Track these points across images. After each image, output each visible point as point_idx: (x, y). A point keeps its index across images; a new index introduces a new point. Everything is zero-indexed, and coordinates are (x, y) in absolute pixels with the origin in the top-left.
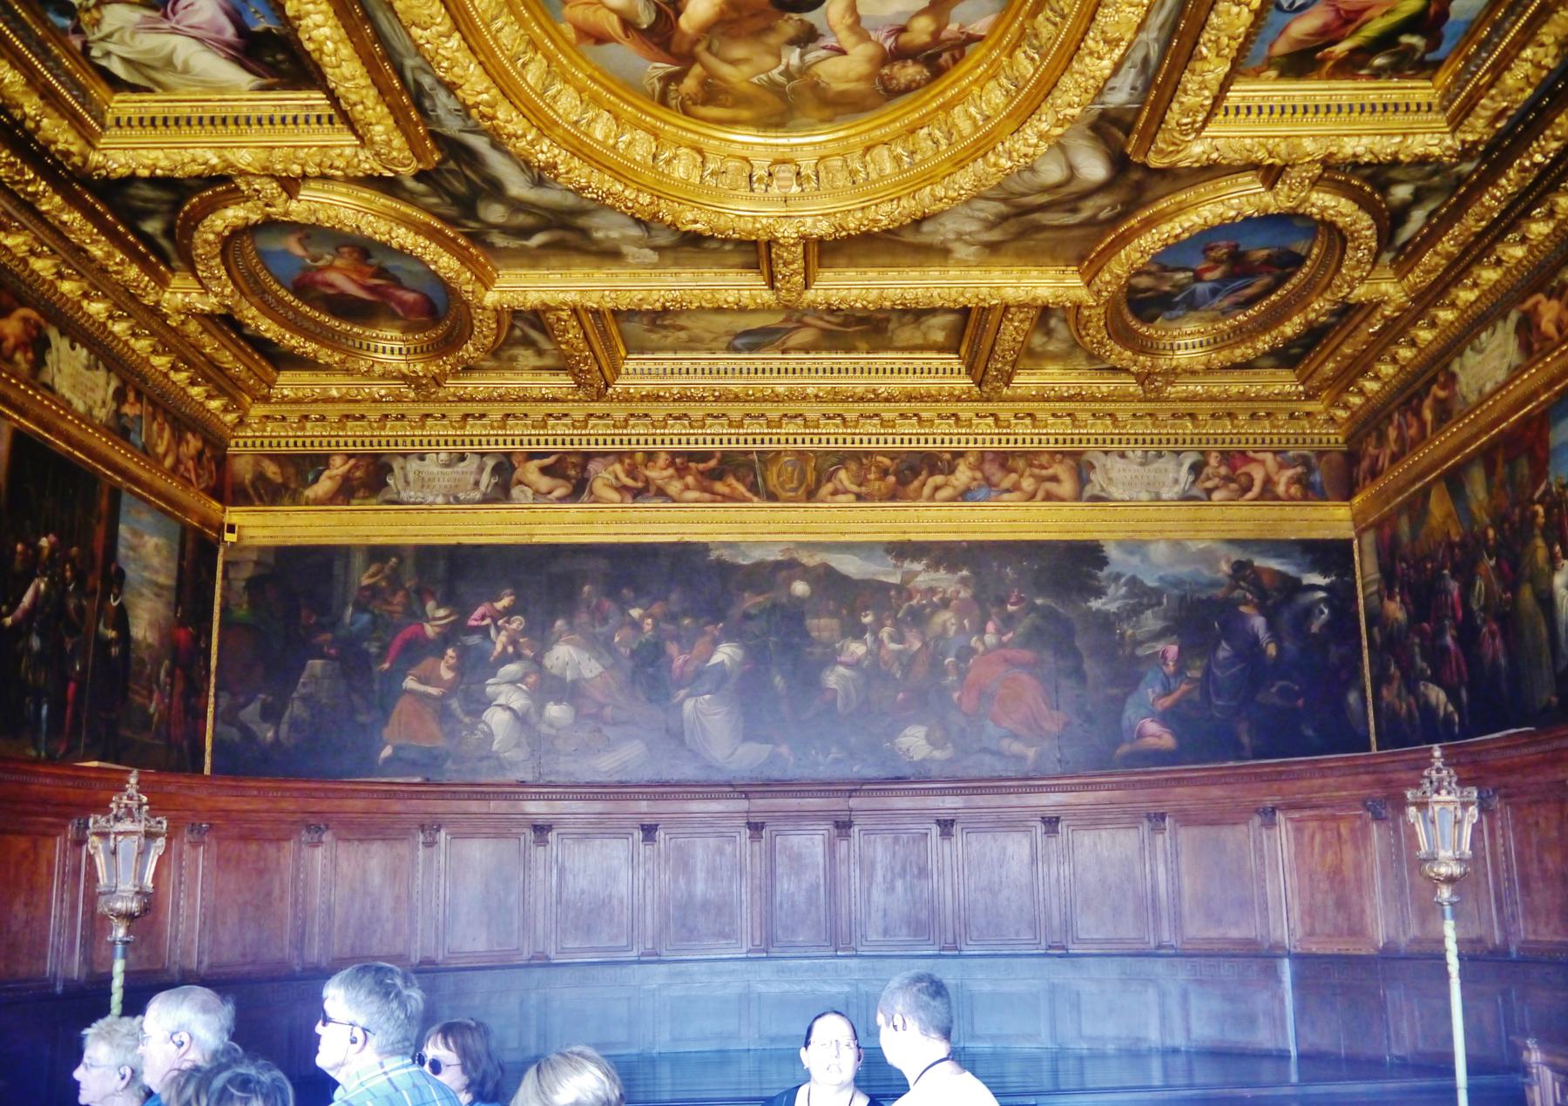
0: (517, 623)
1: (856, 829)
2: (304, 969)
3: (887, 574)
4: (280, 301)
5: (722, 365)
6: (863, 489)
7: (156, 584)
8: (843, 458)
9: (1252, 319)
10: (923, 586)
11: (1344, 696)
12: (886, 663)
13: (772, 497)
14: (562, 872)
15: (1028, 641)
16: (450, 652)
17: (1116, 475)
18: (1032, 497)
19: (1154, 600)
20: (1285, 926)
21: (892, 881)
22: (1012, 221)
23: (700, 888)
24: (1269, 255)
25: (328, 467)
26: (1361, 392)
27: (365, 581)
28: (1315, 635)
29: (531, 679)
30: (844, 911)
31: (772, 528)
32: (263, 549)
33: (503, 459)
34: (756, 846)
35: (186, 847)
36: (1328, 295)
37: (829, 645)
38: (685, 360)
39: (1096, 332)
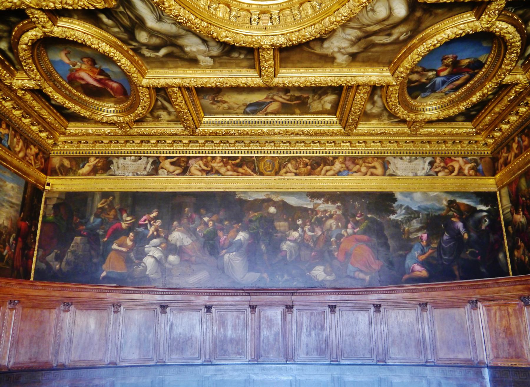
0: (159, 223)
1: (295, 309)
2: (57, 365)
3: (307, 204)
5: (242, 120)
6: (298, 171)
7: (11, 202)
8: (290, 159)
9: (458, 96)
10: (322, 209)
11: (497, 255)
12: (307, 240)
13: (261, 174)
14: (172, 325)
15: (364, 232)
16: (131, 234)
17: (400, 166)
18: (365, 174)
19: (416, 215)
20: (485, 354)
21: (310, 331)
22: (363, 41)
23: (229, 333)
24: (469, 62)
25: (88, 161)
26: (501, 130)
27: (100, 206)
28: (483, 230)
29: (163, 245)
30: (290, 344)
31: (261, 186)
32: (61, 193)
33: (156, 159)
34: (253, 316)
35: (7, 310)
36: (494, 80)
37: (284, 232)
38: (227, 118)
39: (394, 100)
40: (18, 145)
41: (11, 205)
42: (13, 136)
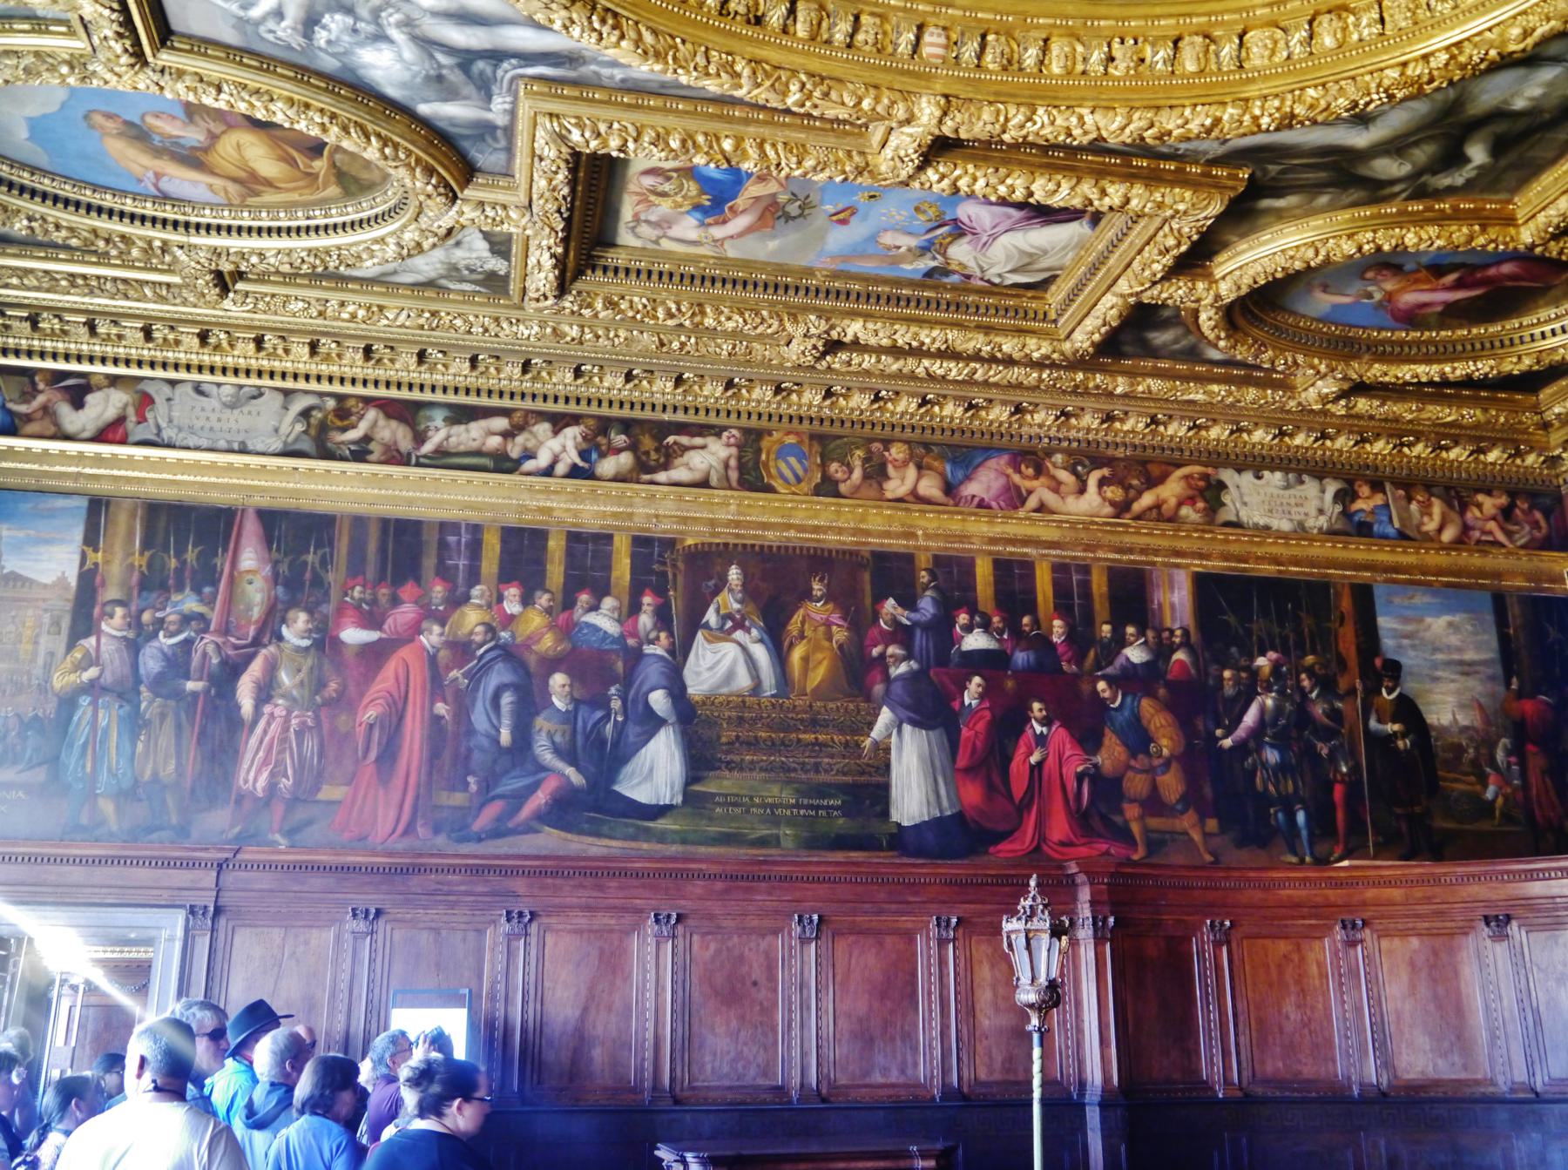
4: (1401, 343)
7: (1461, 663)
40: (1430, 515)
41: (1466, 669)
42: (1404, 503)
